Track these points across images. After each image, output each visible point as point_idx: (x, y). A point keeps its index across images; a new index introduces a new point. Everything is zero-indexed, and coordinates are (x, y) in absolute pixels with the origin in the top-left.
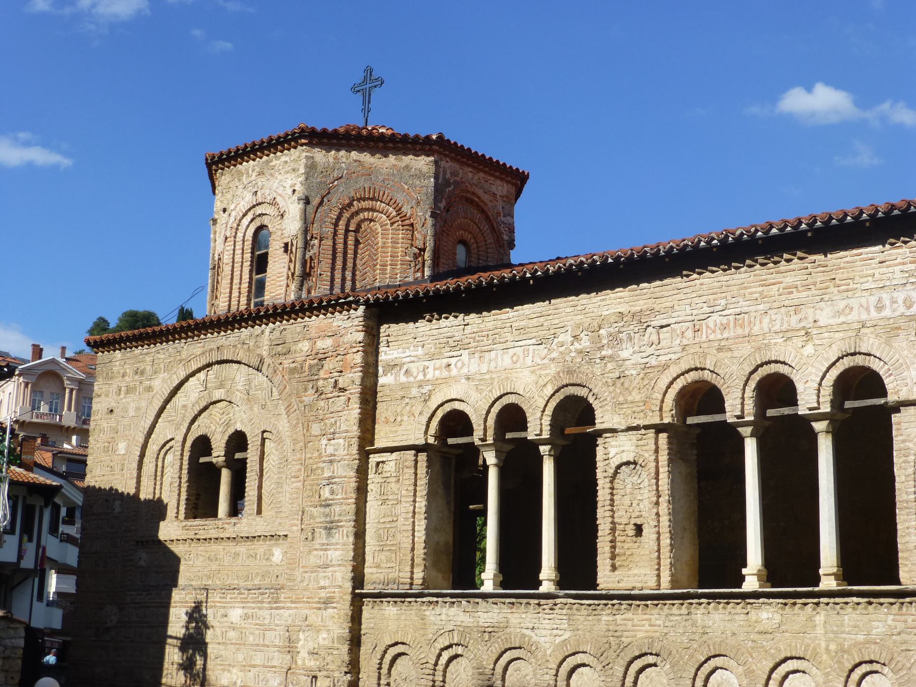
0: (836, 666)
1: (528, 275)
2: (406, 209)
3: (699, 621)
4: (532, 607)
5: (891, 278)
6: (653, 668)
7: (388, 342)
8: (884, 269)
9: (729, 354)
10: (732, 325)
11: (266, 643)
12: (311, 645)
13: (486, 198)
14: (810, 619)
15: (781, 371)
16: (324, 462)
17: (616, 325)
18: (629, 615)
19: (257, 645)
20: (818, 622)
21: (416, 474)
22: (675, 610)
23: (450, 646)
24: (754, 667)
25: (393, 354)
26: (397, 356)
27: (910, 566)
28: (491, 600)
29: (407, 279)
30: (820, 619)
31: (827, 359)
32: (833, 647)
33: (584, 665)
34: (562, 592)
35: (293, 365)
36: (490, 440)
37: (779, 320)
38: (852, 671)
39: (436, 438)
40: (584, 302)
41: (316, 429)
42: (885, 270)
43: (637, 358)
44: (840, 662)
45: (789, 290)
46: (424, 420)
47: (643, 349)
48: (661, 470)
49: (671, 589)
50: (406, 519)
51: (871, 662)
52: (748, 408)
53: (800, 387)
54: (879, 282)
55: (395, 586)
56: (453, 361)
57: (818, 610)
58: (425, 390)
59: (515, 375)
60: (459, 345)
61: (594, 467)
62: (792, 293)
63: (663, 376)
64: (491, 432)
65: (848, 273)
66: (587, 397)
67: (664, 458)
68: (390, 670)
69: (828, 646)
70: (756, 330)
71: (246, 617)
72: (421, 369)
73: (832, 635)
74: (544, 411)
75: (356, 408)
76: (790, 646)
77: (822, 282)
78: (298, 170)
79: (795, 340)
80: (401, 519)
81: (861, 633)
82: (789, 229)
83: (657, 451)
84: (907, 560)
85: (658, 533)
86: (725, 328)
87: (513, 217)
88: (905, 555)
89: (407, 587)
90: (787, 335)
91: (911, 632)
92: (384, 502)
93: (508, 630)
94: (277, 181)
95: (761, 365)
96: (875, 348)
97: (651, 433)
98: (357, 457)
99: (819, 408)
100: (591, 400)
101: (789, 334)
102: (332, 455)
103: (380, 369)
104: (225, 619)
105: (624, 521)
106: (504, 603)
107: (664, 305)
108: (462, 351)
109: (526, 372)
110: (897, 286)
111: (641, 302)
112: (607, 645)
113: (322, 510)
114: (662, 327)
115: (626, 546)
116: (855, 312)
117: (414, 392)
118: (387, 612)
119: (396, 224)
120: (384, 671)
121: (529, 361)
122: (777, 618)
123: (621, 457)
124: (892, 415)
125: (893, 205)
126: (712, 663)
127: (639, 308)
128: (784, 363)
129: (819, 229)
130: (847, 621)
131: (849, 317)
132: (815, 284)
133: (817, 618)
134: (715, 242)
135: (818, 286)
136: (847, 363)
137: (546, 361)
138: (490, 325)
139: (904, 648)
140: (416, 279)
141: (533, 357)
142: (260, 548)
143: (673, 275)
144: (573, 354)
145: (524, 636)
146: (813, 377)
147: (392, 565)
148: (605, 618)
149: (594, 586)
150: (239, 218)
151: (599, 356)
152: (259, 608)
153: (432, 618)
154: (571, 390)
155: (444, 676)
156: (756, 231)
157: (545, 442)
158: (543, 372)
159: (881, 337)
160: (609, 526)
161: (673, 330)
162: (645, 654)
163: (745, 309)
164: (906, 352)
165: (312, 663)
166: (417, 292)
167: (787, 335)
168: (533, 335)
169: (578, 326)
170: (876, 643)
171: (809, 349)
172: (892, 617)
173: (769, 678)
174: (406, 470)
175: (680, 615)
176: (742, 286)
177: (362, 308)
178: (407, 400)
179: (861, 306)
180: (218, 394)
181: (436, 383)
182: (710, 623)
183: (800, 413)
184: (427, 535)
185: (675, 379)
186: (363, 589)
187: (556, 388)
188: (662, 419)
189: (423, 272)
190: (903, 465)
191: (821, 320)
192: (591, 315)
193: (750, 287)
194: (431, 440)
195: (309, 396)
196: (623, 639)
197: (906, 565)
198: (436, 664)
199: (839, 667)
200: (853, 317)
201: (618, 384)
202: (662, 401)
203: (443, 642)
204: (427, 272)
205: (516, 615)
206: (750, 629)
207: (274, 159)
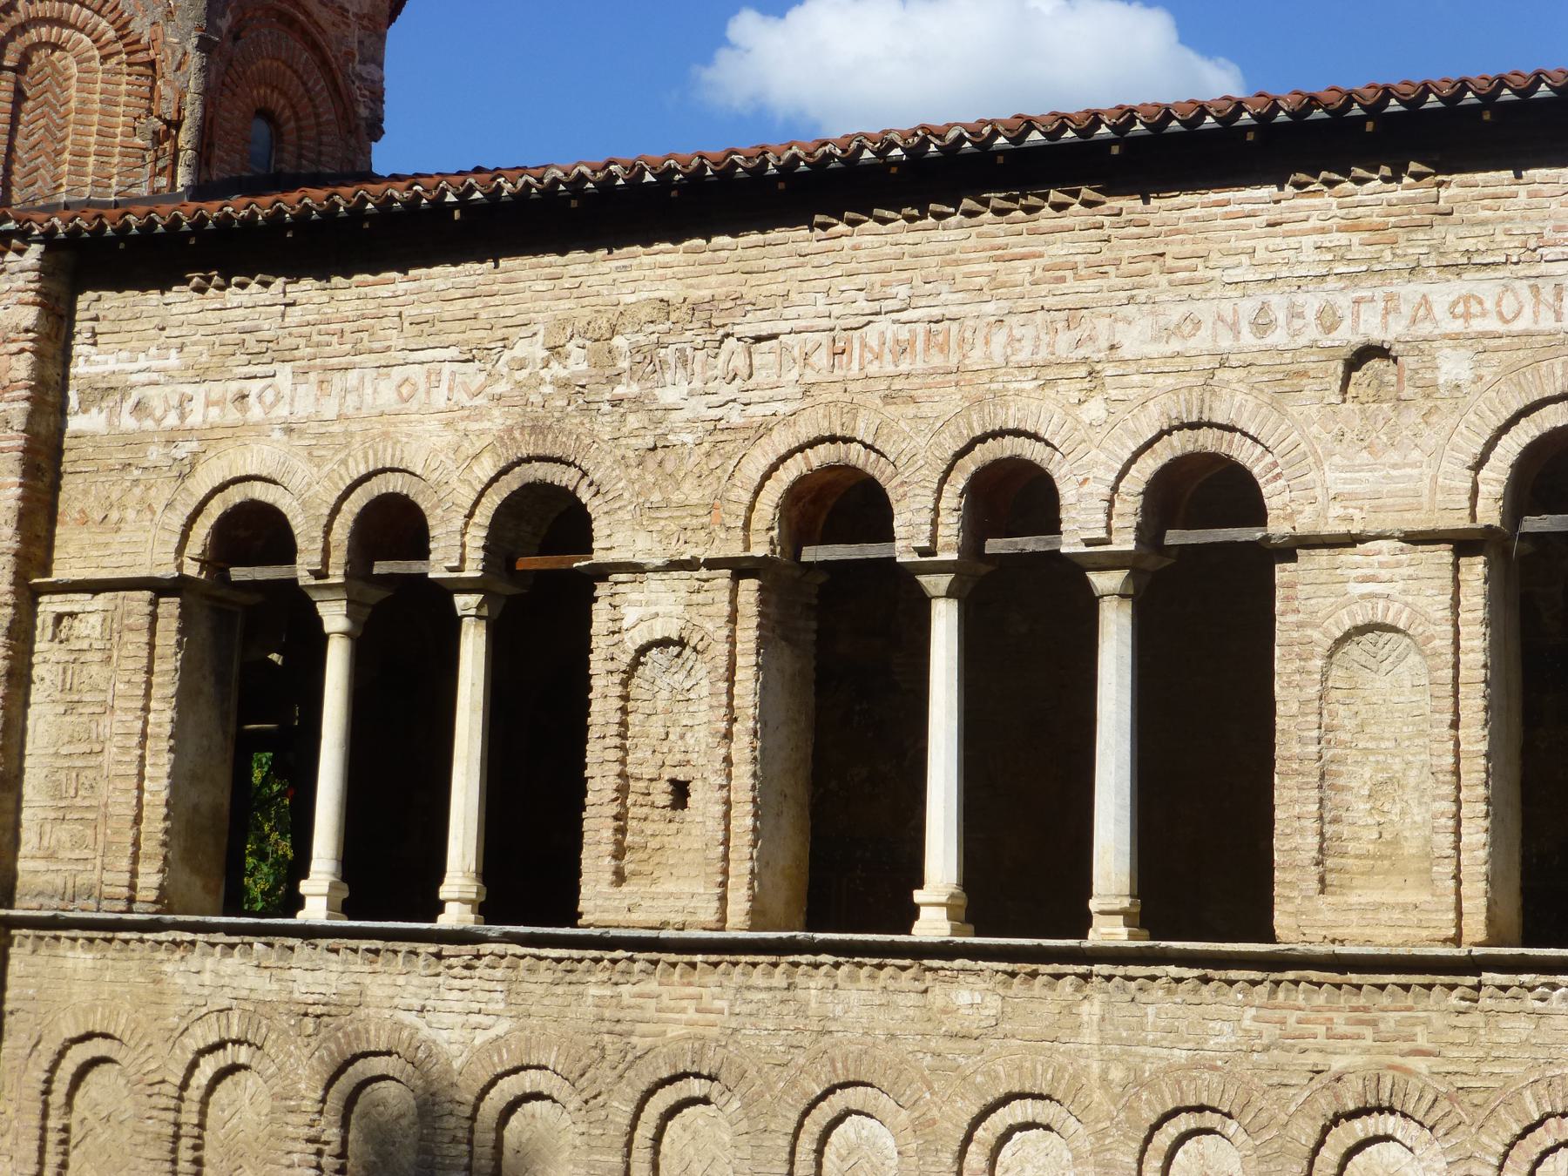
0: (1122, 1116)
1: (450, 198)
2: (141, 27)
3: (813, 1004)
4: (421, 961)
5: (1293, 260)
6: (701, 1108)
7: (94, 334)
8: (1278, 240)
9: (911, 410)
10: (920, 345)
13: (324, 16)
14: (1069, 1009)
15: (1028, 455)
17: (652, 328)
18: (651, 986)
20: (1085, 1018)
21: (152, 646)
22: (757, 977)
23: (221, 1045)
24: (935, 1113)
25: (106, 363)
26: (117, 367)
27: (1298, 901)
28: (323, 943)
29: (134, 191)
30: (1091, 1010)
31: (1134, 434)
32: (1116, 1074)
33: (538, 1096)
34: (495, 930)
36: (337, 576)
38: (1156, 1127)
39: (204, 563)
40: (579, 269)
42: (1273, 243)
43: (699, 408)
44: (1131, 1108)
45: (1058, 272)
46: (177, 520)
47: (712, 386)
48: (740, 661)
49: (750, 930)
50: (124, 749)
51: (1200, 1109)
52: (947, 532)
53: (1067, 492)
54: (1266, 268)
55: (92, 903)
56: (254, 387)
57: (1088, 989)
58: (184, 450)
59: (405, 428)
60: (270, 352)
61: (585, 648)
62: (1062, 280)
63: (756, 452)
64: (339, 558)
65: (1195, 243)
66: (576, 488)
67: (748, 634)
68: (70, 1096)
69: (1105, 1071)
70: (976, 358)
72: (174, 401)
73: (1116, 1049)
74: (470, 515)
75: (12, 485)
76: (1020, 1068)
79: (1063, 386)
80: (112, 750)
81: (1180, 1046)
82: (1069, 134)
83: (733, 618)
84: (1292, 889)
85: (727, 803)
86: (903, 349)
87: (381, 66)
88: (1289, 877)
89: (122, 905)
90: (1046, 373)
91: (1293, 1046)
92: (71, 708)
93: (362, 1013)
95: (982, 439)
96: (1246, 415)
97: (723, 578)
98: (9, 599)
99: (1109, 542)
100: (584, 495)
101: (1051, 373)
103: (73, 398)
105: (648, 771)
106: (355, 951)
107: (765, 290)
108: (276, 366)
109: (433, 424)
110: (1304, 281)
111: (713, 280)
112: (596, 1054)
114: (758, 339)
115: (649, 828)
116: (1205, 332)
117: (155, 454)
118: (69, 964)
119: (114, 60)
120: (57, 1098)
121: (439, 398)
122: (993, 1004)
123: (651, 629)
124: (1277, 567)
125: (1312, 98)
126: (838, 1101)
127: (706, 294)
128: (1036, 437)
129: (1138, 139)
130: (1151, 1019)
131: (1192, 342)
132: (1117, 263)
133: (1085, 1008)
134: (897, 152)
135: (1124, 267)
136: (1179, 444)
137: (478, 401)
138: (348, 309)
139: (1275, 1080)
140: (156, 192)
141: (450, 389)
143: (791, 221)
144: (547, 389)
145: (399, 1026)
146: (1100, 472)
147: (87, 853)
148: (593, 991)
149: (572, 917)
151: (608, 396)
153: (180, 980)
154: (539, 472)
155: (203, 1113)
156: (995, 134)
157: (468, 587)
159: (1261, 391)
160: (613, 782)
161: (786, 349)
162: (685, 1075)
163: (953, 311)
164: (1315, 429)
166: (177, 219)
167: (1046, 373)
168: (453, 338)
169: (562, 324)
170: (1215, 1068)
171: (1095, 409)
172: (1253, 1011)
173: (968, 1139)
174: (128, 636)
175: (770, 989)
176: (950, 258)
177: (35, 250)
178: (136, 473)
179: (1220, 318)
181: (210, 437)
182: (839, 1010)
183: (1063, 550)
184: (174, 788)
185: (783, 459)
186: (11, 906)
187: (502, 464)
188: (747, 548)
189: (174, 176)
190: (1297, 677)
191: (1126, 344)
192: (593, 300)
193: (968, 262)
194: (192, 569)
196: (634, 1040)
197: (1289, 899)
198: (184, 1086)
199: (1128, 1119)
200: (1201, 342)
201: (651, 463)
202: (751, 508)
204: (183, 178)
205: (380, 979)
206: (929, 1026)
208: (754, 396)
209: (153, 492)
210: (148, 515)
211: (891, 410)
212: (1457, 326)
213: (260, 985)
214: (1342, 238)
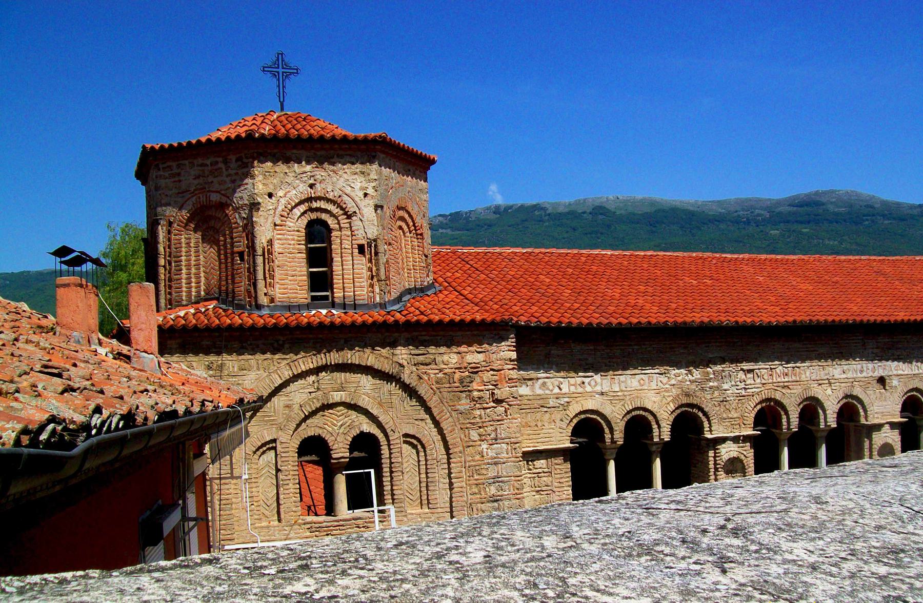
9: (789, 391)
16: (488, 464)
35: (441, 375)
41: (474, 435)
56: (587, 380)
72: (557, 383)
77: (837, 353)
78: (369, 175)
79: (823, 385)
94: (342, 179)
102: (495, 458)
109: (651, 394)
116: (851, 373)
117: (552, 403)
131: (848, 375)
136: (845, 401)
150: (289, 207)
151: (708, 386)
158: (666, 394)
171: (829, 392)
180: (337, 397)
191: (835, 375)
195: (464, 404)
200: (850, 375)
207: (335, 156)
208: (750, 386)
209: (553, 416)
210: (553, 424)
211: (783, 391)
212: (895, 372)
214: (875, 351)
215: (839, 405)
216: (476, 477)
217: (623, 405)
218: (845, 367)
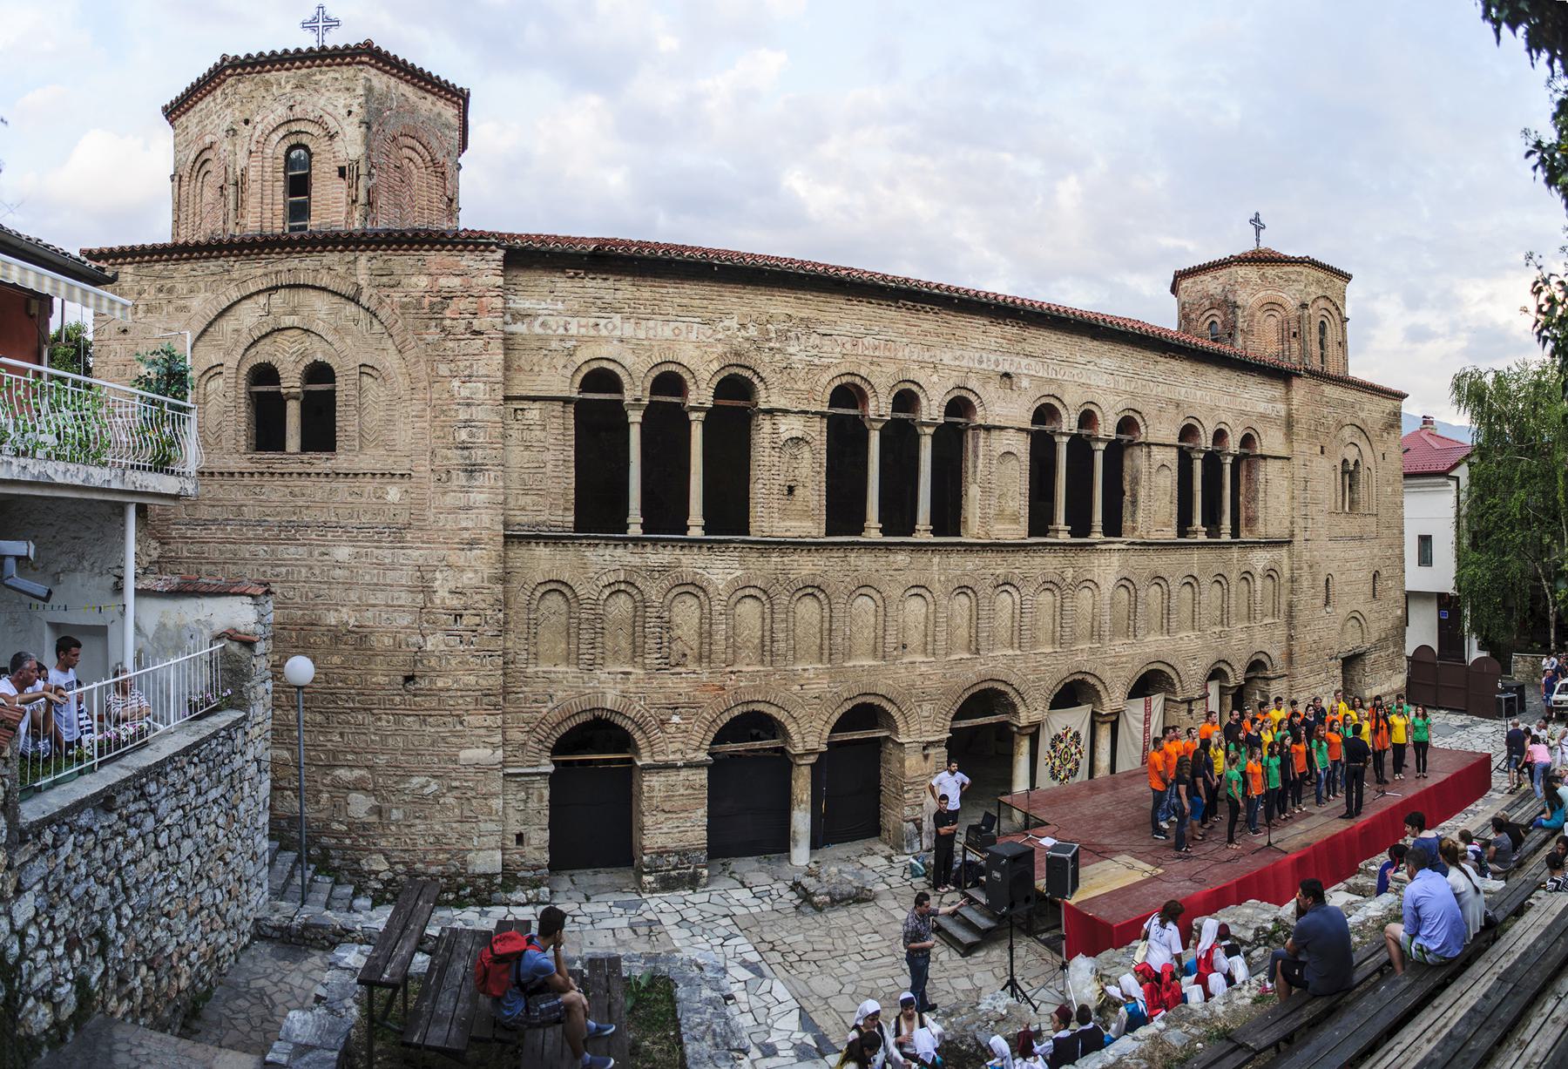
11: (388, 582)
12: (452, 585)
18: (796, 557)
19: (377, 585)
30: (936, 560)
32: (942, 578)
37: (917, 353)
43: (803, 355)
56: (602, 322)
58: (569, 344)
70: (900, 355)
71: (357, 556)
72: (562, 323)
80: (550, 466)
90: (922, 364)
104: (326, 557)
109: (690, 346)
113: (459, 452)
117: (554, 345)
121: (693, 337)
136: (956, 393)
142: (369, 486)
152: (377, 548)
165: (455, 602)
167: (922, 364)
169: (745, 316)
171: (935, 378)
176: (892, 321)
181: (581, 340)
200: (964, 363)
203: (605, 580)
213: (636, 560)
214: (1000, 340)
215: (949, 398)
216: (442, 418)
217: (650, 357)
218: (958, 353)
